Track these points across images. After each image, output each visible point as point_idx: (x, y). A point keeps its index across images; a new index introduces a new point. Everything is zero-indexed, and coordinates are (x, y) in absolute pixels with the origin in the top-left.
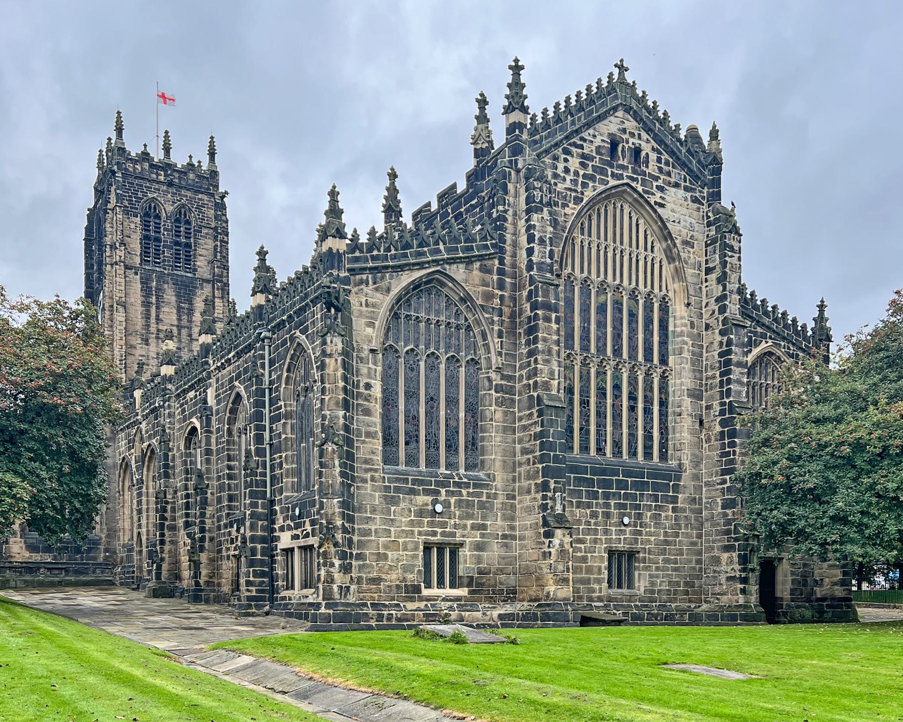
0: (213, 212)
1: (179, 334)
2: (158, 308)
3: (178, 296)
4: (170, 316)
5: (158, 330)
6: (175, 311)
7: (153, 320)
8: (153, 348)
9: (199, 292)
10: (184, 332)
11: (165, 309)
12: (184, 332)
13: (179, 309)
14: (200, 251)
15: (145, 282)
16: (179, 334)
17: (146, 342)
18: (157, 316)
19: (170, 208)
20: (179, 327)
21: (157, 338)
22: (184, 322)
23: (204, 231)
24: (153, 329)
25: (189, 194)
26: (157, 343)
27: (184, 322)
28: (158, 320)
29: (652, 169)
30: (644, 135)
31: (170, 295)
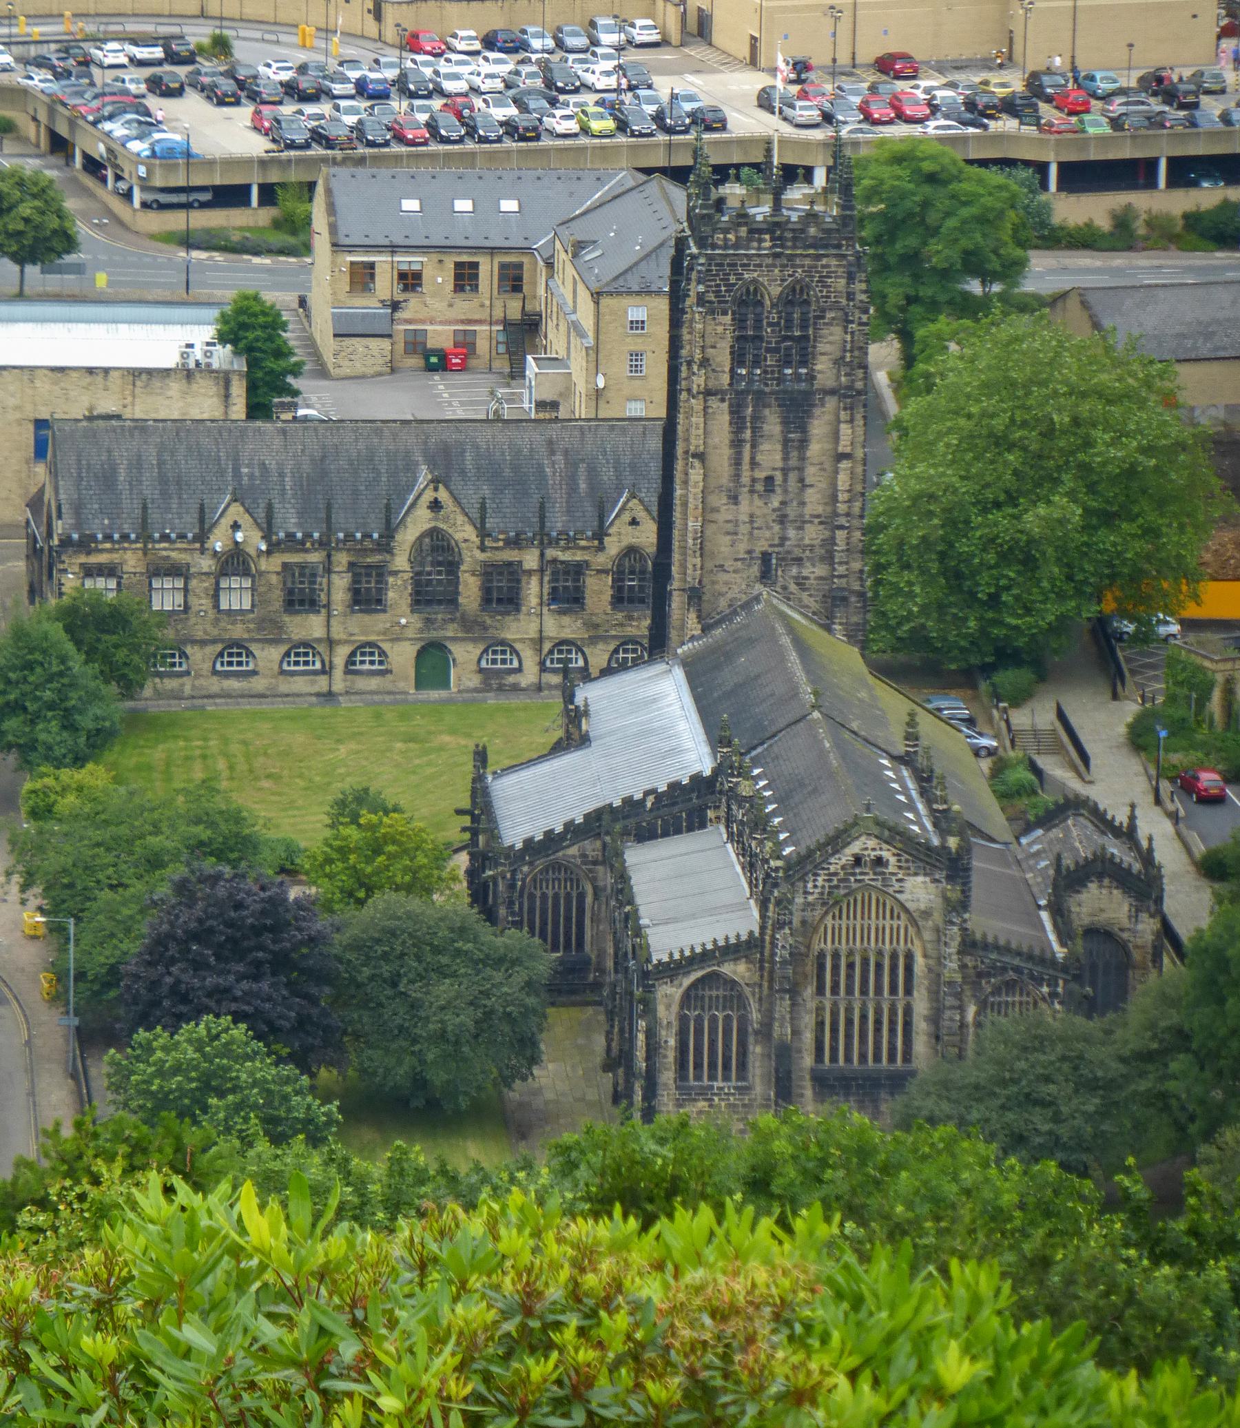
0: (843, 282)
1: (785, 480)
2: (753, 446)
3: (785, 422)
4: (771, 455)
5: (754, 480)
6: (779, 447)
7: (746, 466)
8: (745, 507)
9: (817, 411)
10: (793, 476)
11: (765, 446)
12: (793, 476)
13: (786, 442)
14: (821, 347)
15: (736, 412)
16: (785, 480)
17: (734, 499)
18: (753, 458)
19: (776, 290)
20: (785, 471)
21: (752, 492)
22: (793, 462)
23: (829, 315)
24: (745, 479)
25: (807, 262)
26: (752, 502)
27: (793, 462)
28: (754, 464)
29: (891, 869)
30: (885, 846)
31: (773, 424)
